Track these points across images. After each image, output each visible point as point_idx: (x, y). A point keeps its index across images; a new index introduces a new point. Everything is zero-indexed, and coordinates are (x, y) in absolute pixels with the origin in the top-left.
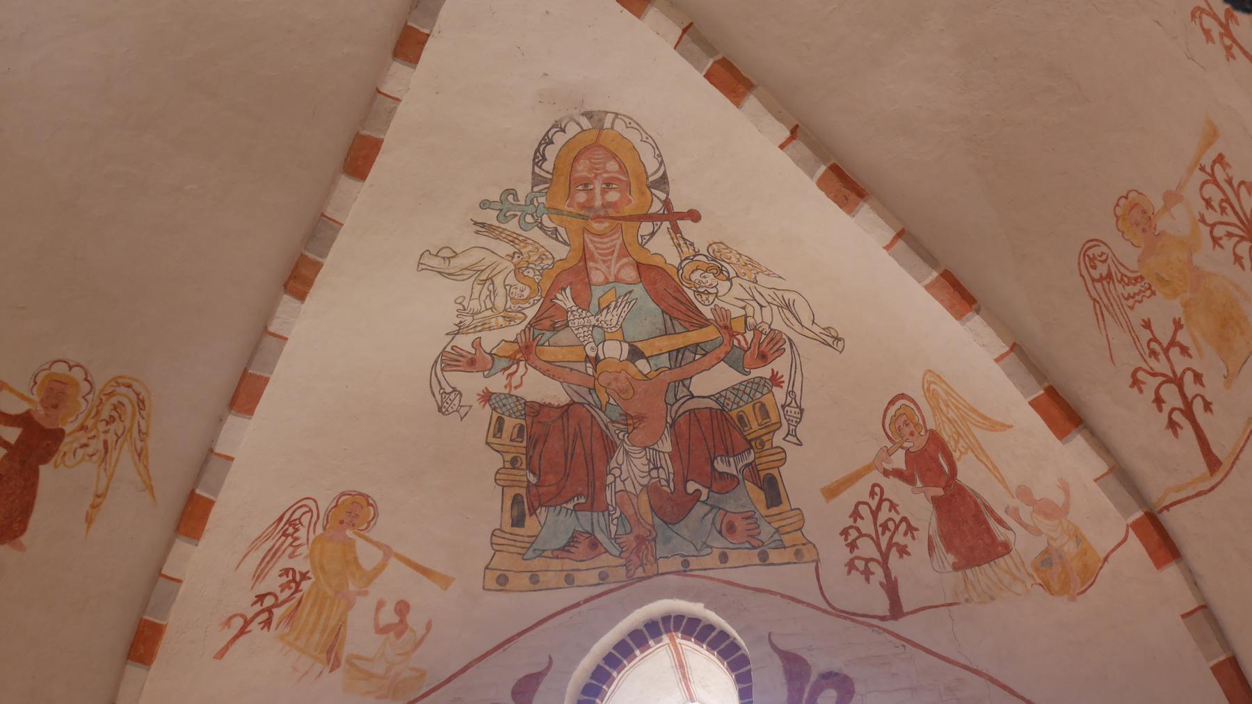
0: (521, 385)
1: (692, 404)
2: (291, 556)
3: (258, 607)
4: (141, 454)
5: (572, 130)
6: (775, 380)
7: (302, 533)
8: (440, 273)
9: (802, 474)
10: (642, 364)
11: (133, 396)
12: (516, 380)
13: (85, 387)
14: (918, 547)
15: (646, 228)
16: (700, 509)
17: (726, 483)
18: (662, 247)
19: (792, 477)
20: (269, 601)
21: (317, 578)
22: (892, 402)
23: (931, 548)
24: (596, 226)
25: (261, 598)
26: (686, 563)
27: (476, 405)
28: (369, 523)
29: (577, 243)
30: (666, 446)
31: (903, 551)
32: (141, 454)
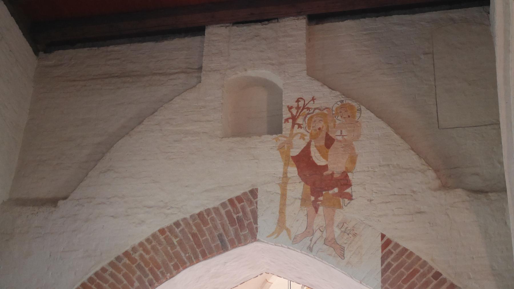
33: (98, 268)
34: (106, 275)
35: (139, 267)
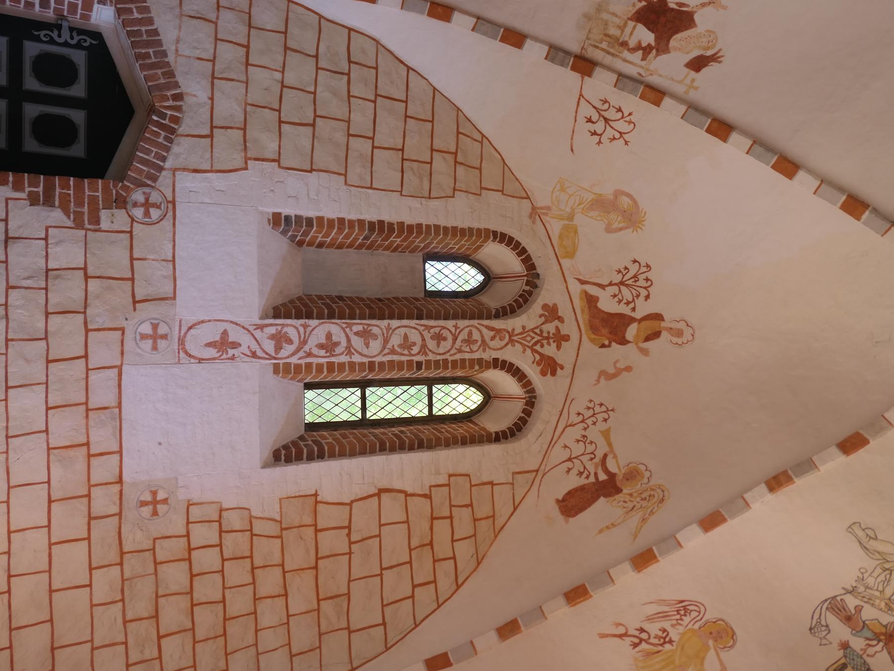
0: (872, 656)
2: (673, 626)
3: (637, 633)
4: (644, 520)
7: (687, 619)
8: (860, 543)
11: (661, 496)
12: (871, 651)
13: (646, 480)
20: (644, 636)
21: (677, 649)
25: (642, 630)
27: (835, 645)
28: (725, 647)
32: (644, 520)
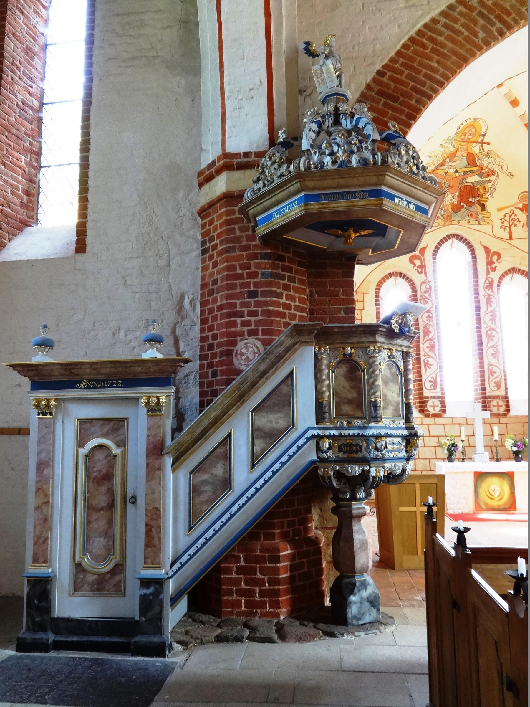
1: (466, 184)
5: (469, 121)
6: (490, 181)
9: (492, 204)
10: (457, 174)
14: (520, 225)
15: (475, 144)
16: (463, 210)
17: (471, 204)
18: (476, 149)
19: (488, 205)
22: (523, 193)
23: (523, 226)
24: (463, 144)
26: (459, 222)
29: (457, 148)
30: (457, 193)
31: (515, 225)
33: (427, 19)
34: (439, 27)
35: (480, 14)
